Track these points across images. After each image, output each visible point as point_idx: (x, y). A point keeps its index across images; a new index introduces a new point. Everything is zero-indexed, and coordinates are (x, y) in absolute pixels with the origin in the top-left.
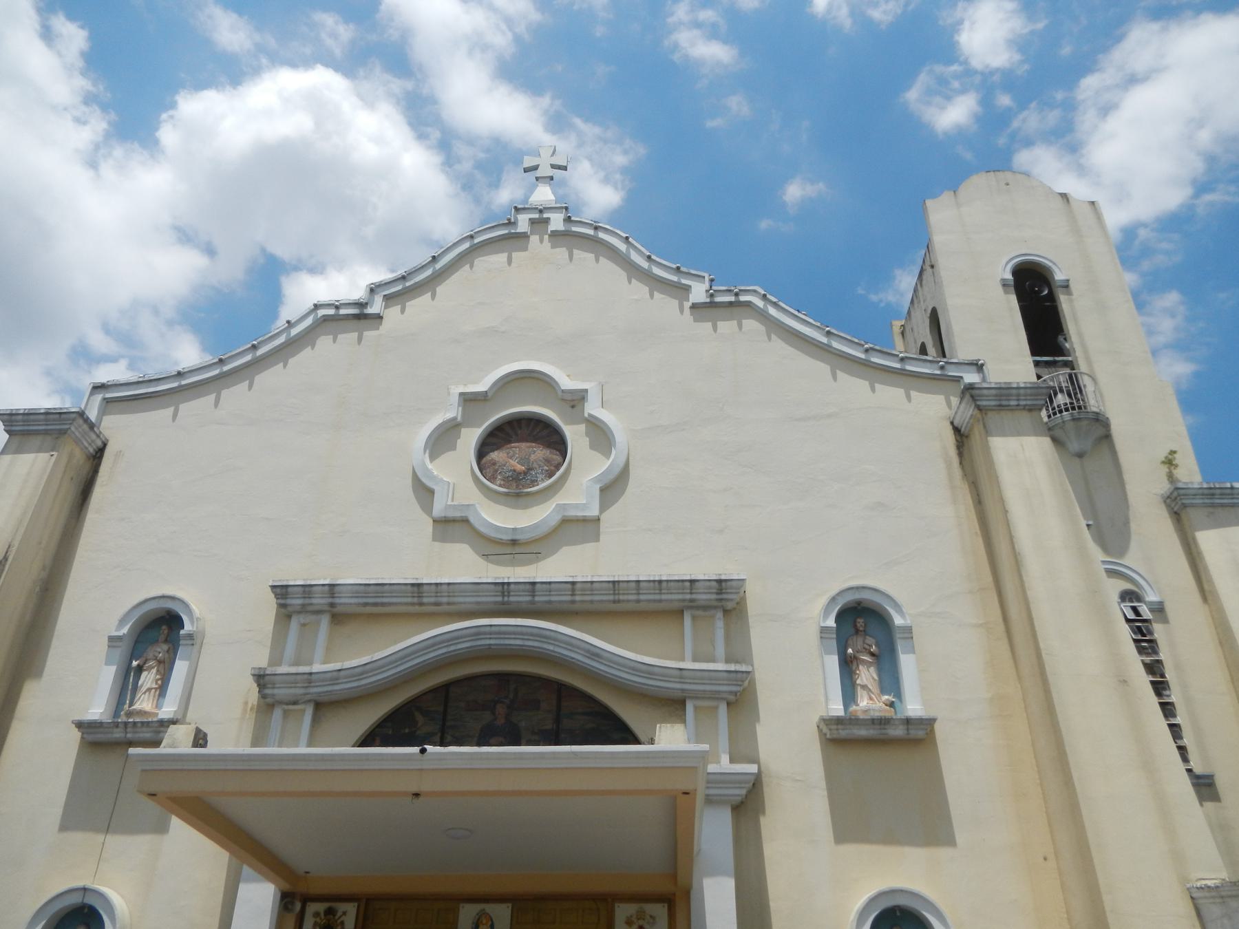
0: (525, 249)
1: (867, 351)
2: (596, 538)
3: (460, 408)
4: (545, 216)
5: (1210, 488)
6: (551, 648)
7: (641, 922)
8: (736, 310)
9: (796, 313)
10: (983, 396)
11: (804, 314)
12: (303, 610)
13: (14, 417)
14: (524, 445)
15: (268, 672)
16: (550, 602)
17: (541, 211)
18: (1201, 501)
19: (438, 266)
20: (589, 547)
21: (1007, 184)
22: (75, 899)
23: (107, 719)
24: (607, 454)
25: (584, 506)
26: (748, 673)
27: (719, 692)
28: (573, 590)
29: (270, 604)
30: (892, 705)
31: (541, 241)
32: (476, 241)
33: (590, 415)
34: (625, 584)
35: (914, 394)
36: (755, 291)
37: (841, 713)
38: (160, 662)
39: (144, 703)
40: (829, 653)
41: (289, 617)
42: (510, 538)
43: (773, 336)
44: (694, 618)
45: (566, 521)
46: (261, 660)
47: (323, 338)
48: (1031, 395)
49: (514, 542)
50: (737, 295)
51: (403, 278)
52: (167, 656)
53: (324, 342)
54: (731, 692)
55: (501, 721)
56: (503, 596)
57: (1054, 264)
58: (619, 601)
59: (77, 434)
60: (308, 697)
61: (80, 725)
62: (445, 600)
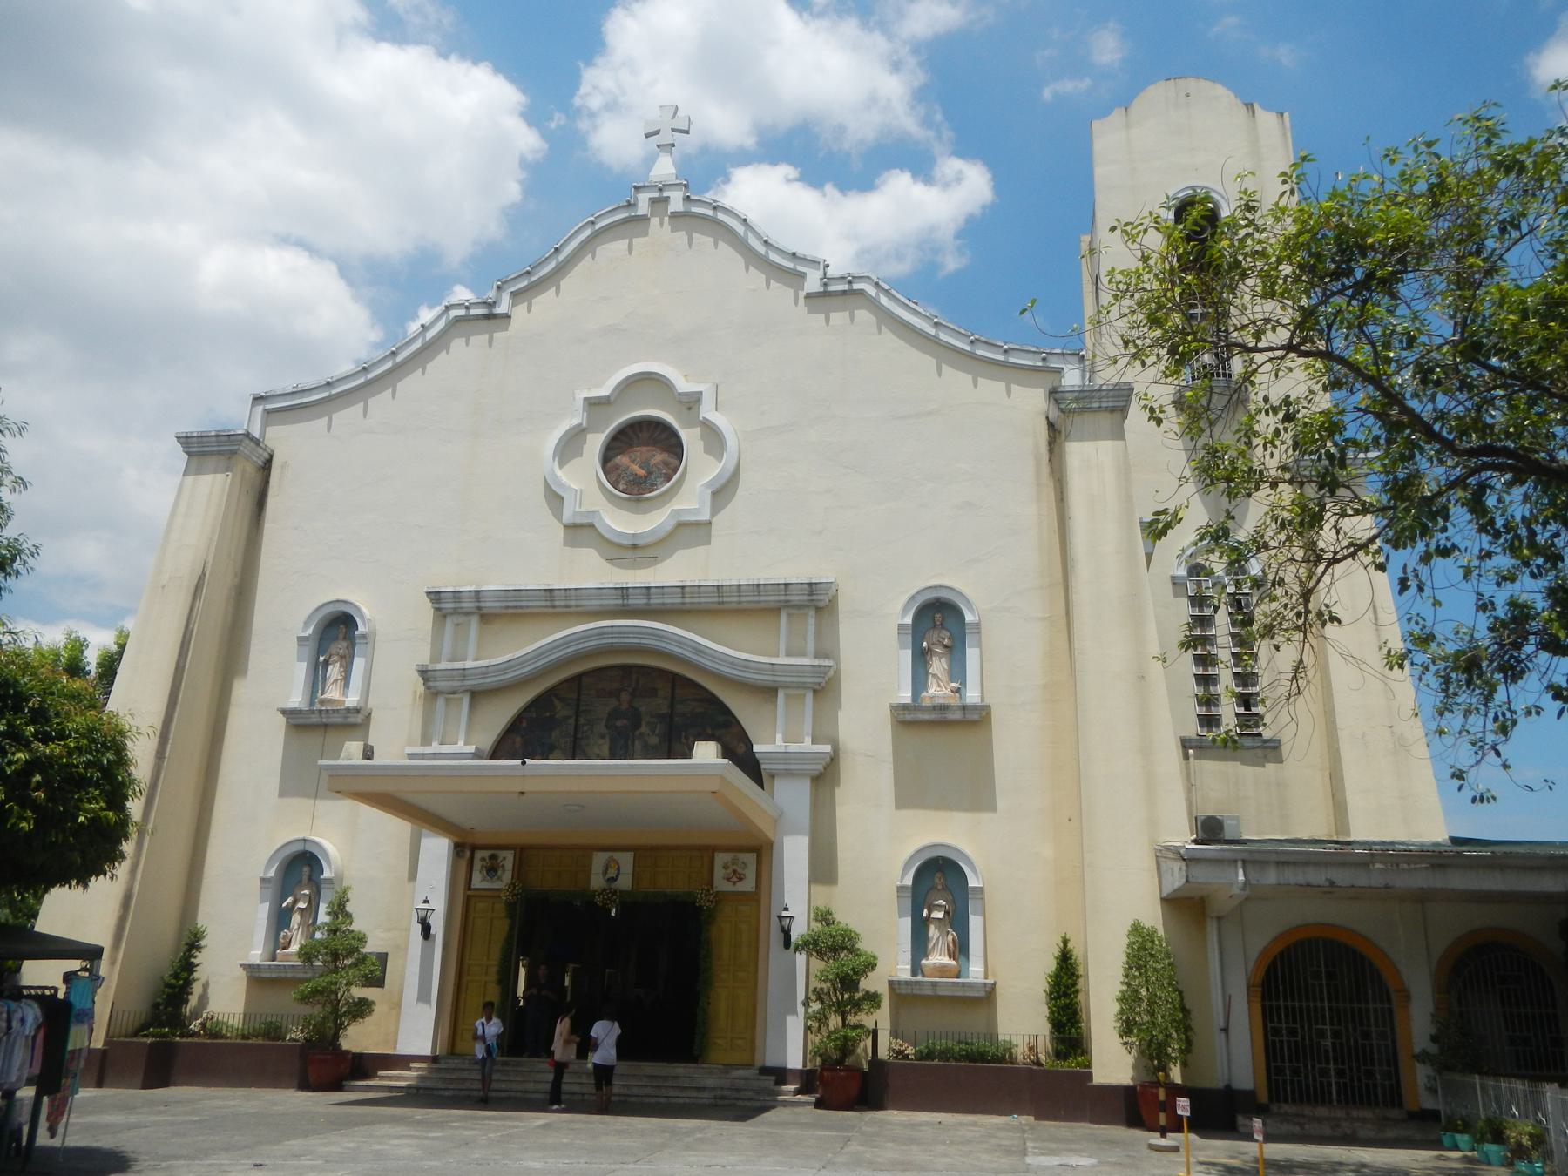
0: (646, 234)
2: (708, 543)
4: (665, 194)
6: (664, 645)
7: (735, 867)
9: (907, 302)
11: (916, 304)
12: (455, 612)
14: (644, 449)
15: (429, 668)
16: (663, 604)
19: (561, 257)
20: (701, 549)
21: (1188, 95)
22: (299, 847)
23: (305, 707)
24: (719, 457)
25: (697, 511)
27: (805, 683)
28: (683, 593)
29: (427, 610)
30: (958, 691)
31: (661, 224)
35: (1014, 387)
36: (868, 277)
37: (909, 701)
38: (342, 657)
39: (333, 693)
40: (902, 647)
41: (445, 616)
42: (631, 543)
43: (883, 327)
44: (789, 615)
45: (680, 525)
46: (424, 656)
47: (456, 340)
48: (1113, 397)
49: (635, 547)
50: (850, 282)
53: (458, 344)
55: (625, 706)
56: (623, 599)
57: (1223, 198)
58: (723, 603)
60: (464, 688)
61: (284, 712)
62: (573, 603)
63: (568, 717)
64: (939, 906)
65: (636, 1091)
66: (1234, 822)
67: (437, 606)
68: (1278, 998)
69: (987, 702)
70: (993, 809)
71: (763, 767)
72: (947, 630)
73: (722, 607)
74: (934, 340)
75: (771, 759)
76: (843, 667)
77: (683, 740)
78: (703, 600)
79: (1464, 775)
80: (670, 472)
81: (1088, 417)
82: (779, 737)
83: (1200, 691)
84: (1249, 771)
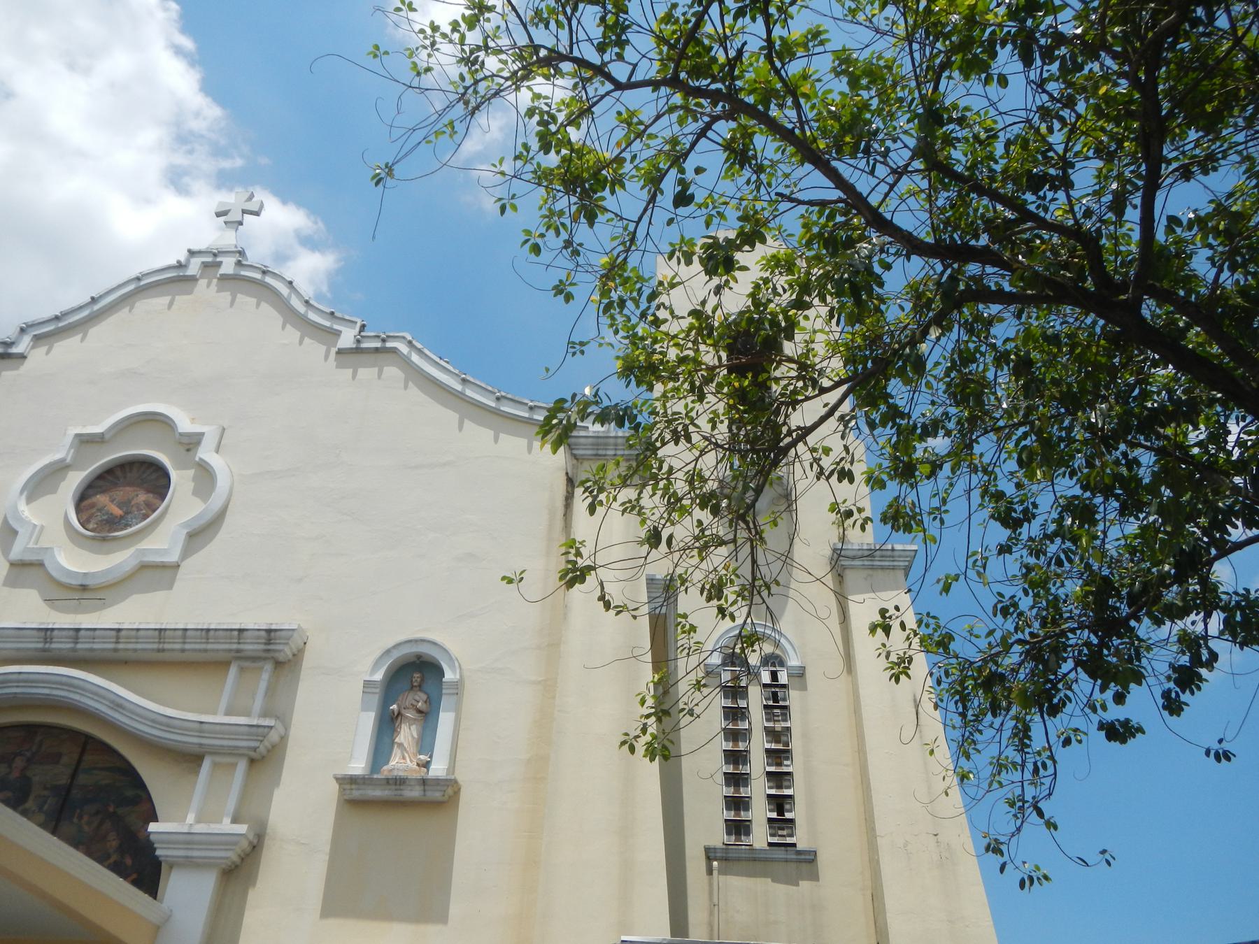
1: (498, 399)
2: (170, 587)
3: (72, 451)
4: (219, 259)
5: (871, 550)
6: (77, 697)
8: (380, 356)
9: (438, 360)
10: (580, 444)
16: (92, 650)
17: (215, 255)
18: (860, 563)
19: (96, 307)
20: (160, 595)
25: (165, 552)
26: (271, 727)
28: (118, 638)
31: (209, 285)
32: (142, 283)
33: (201, 459)
34: (171, 633)
36: (404, 338)
40: (365, 708)
42: (79, 583)
43: (410, 383)
44: (242, 670)
45: (144, 567)
49: (84, 588)
50: (384, 341)
51: (57, 318)
54: (249, 748)
55: (15, 774)
58: (163, 650)
69: (459, 776)
70: (443, 918)
71: (158, 853)
72: (426, 693)
73: (160, 656)
74: (460, 396)
75: (169, 842)
76: (293, 732)
77: (75, 820)
78: (139, 646)
79: (1004, 848)
82: (191, 818)
83: (730, 791)
84: (781, 889)
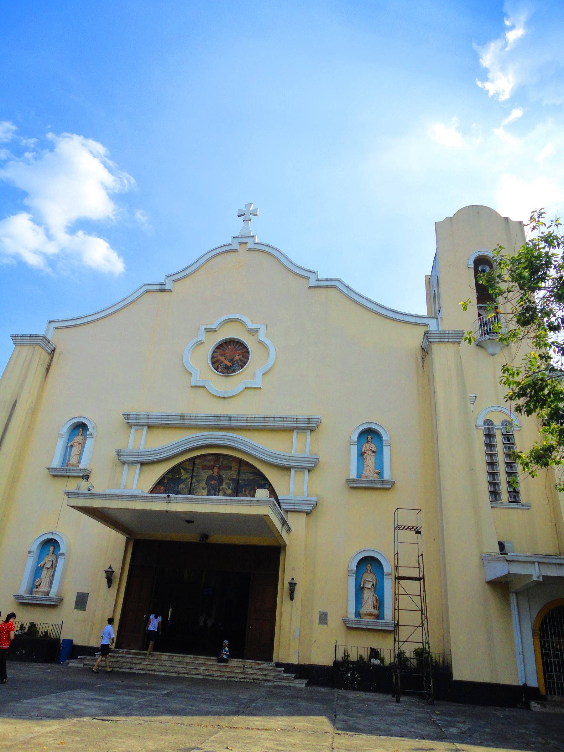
6: (236, 445)
12: (136, 425)
13: (17, 338)
30: (379, 473)
41: (131, 427)
44: (298, 433)
45: (247, 388)
52: (82, 441)
59: (43, 345)
61: (49, 469)
63: (188, 478)
64: (369, 581)
65: (211, 673)
66: (510, 545)
67: (127, 421)
68: (548, 638)
77: (244, 492)
80: (242, 364)
81: (443, 346)
